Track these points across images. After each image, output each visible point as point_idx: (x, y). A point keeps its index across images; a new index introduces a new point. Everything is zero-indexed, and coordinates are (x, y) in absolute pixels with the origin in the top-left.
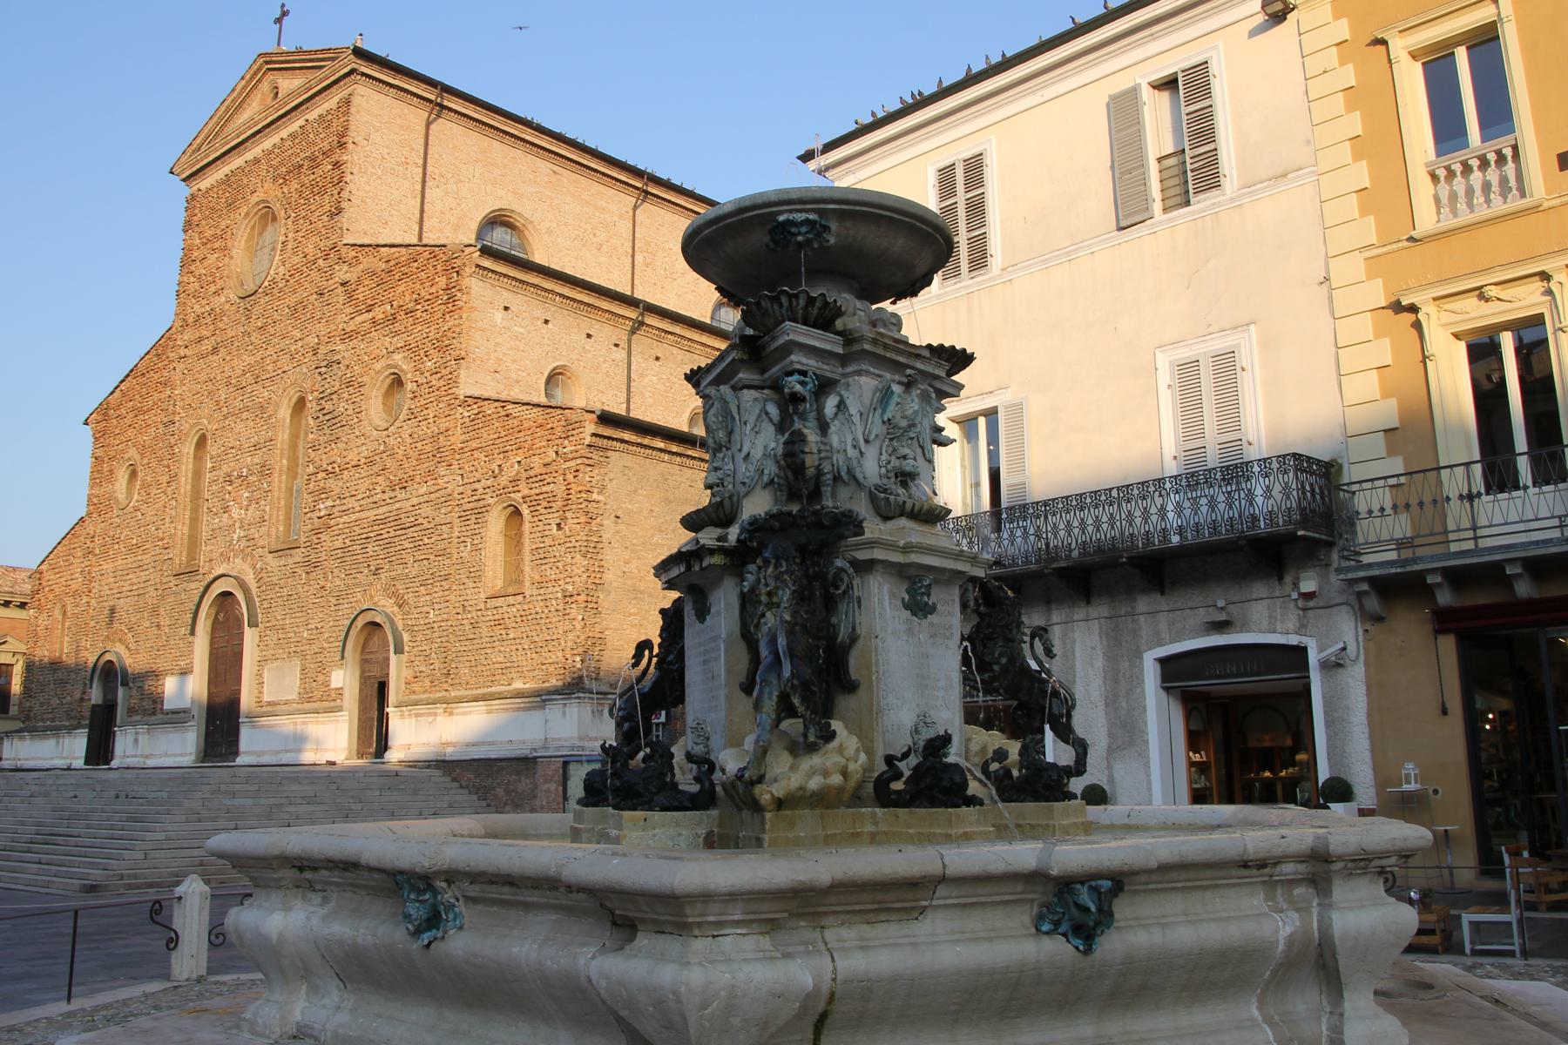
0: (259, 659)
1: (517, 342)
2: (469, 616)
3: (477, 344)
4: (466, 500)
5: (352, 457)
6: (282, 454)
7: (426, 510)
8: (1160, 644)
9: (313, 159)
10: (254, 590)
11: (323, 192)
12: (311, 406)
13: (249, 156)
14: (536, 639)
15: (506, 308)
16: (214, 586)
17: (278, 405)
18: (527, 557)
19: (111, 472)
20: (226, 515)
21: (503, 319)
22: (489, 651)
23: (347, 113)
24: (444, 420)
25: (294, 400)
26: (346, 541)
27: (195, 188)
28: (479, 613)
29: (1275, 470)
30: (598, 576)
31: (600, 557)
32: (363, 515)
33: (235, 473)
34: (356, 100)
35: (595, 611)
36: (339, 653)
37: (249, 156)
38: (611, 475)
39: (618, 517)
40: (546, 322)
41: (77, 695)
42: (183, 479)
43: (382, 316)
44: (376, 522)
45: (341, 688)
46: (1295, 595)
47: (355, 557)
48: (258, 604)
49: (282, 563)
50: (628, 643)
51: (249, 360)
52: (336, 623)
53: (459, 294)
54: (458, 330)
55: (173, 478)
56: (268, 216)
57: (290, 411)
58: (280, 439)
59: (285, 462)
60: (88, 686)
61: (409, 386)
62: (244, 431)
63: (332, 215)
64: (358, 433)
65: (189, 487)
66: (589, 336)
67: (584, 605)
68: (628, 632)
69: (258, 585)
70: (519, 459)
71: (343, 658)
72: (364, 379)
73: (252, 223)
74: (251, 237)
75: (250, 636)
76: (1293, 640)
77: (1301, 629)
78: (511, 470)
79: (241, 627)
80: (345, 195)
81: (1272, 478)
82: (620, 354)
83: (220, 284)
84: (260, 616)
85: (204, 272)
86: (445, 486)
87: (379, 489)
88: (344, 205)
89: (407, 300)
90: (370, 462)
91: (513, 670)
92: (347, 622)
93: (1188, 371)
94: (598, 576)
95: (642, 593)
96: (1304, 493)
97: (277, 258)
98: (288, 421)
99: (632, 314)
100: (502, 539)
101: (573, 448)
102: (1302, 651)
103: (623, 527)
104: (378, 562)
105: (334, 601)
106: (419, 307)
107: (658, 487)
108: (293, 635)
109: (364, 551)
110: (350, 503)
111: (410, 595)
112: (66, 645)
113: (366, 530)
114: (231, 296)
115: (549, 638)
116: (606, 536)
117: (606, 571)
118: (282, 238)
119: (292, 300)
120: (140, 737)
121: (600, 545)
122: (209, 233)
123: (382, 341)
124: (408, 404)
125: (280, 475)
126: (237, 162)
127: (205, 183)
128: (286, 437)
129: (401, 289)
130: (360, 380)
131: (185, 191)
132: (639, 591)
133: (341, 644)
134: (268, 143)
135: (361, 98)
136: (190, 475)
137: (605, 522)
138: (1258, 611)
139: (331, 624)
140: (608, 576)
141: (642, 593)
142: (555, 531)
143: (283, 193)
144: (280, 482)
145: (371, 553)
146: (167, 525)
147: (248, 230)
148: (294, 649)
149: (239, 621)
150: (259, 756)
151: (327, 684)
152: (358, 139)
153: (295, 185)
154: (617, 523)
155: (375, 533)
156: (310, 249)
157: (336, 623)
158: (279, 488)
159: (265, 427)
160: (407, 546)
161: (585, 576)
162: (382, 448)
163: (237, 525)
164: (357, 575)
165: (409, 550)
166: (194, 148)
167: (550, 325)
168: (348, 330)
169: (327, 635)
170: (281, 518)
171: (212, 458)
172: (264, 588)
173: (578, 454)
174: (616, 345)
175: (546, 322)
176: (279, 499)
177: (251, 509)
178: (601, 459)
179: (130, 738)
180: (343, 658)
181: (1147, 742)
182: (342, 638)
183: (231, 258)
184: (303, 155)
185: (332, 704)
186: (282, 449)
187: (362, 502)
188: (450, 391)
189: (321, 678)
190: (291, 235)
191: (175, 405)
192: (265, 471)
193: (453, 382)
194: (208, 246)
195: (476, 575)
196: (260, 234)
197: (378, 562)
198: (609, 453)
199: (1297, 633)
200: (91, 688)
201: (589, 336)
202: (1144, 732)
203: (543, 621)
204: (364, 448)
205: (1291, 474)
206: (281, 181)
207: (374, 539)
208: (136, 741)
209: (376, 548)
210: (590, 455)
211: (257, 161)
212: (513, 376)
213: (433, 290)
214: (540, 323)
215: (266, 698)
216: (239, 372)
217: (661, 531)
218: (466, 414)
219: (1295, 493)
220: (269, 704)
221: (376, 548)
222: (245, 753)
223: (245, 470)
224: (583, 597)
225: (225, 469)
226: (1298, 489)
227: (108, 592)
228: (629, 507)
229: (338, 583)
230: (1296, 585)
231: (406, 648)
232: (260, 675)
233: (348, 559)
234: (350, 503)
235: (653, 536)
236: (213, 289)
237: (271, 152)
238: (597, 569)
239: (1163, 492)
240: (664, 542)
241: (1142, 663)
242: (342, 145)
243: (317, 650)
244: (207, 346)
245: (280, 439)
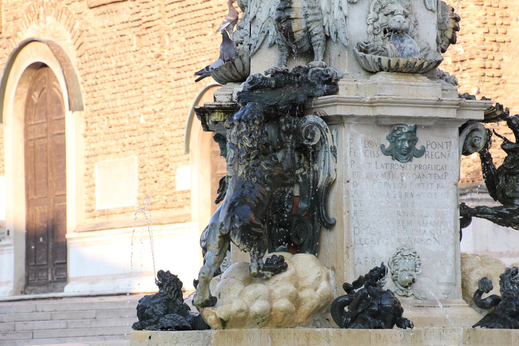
0: (87, 153)
10: (74, 60)
45: (189, 191)
47: (196, 14)
48: (80, 80)
49: (107, 22)
52: (179, 104)
69: (80, 52)
71: (188, 150)
79: (61, 111)
84: (84, 95)
105: (173, 74)
108: (126, 121)
133: (184, 132)
139: (173, 104)
148: (129, 140)
149: (58, 101)
150: (93, 283)
151: (170, 185)
157: (179, 104)
164: (201, 39)
169: (167, 120)
172: (86, 57)
180: (188, 150)
185: (179, 212)
189: (163, 177)
215: (99, 206)
220: (103, 213)
222: (77, 279)
229: (177, 49)
232: (89, 175)
233: (187, 16)
243: (156, 141)
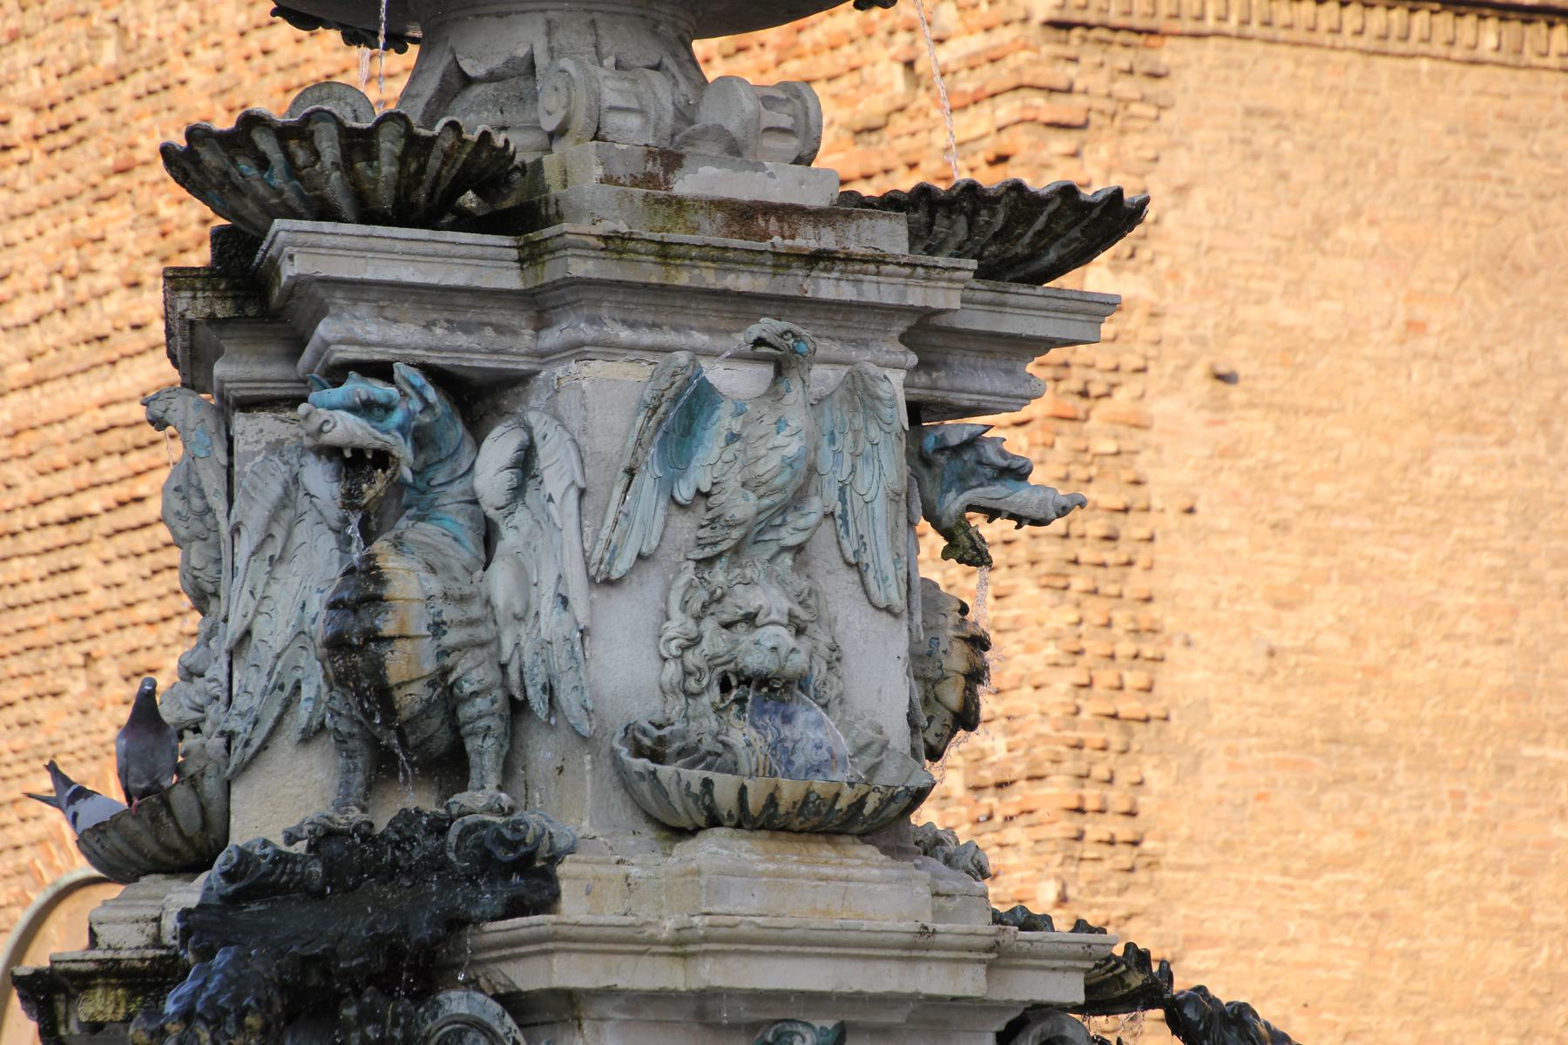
30: (1134, 679)
31: (1137, 582)
32: (44, 402)
35: (1125, 856)
39: (1226, 378)
44: (112, 440)
67: (1069, 825)
68: (1308, 952)
87: (109, 269)
94: (1134, 679)
101: (978, 42)
103: (1257, 425)
104: (131, 638)
107: (1447, 200)
109: (63, 584)
113: (65, 481)
117: (1175, 652)
121: (1133, 528)
132: (1362, 740)
137: (1161, 408)
141: (1381, 749)
145: (97, 597)
154: (1220, 406)
155: (110, 495)
161: (1062, 683)
173: (1001, 76)
178: (1125, 87)
187: (35, 338)
197: (131, 638)
198: (1167, 54)
207: (107, 523)
209: (119, 571)
210: (1062, 74)
217: (1468, 426)
221: (119, 571)
224: (1057, 790)
228: (1288, 317)
235: (1426, 455)
238: (1125, 648)
240: (1488, 486)
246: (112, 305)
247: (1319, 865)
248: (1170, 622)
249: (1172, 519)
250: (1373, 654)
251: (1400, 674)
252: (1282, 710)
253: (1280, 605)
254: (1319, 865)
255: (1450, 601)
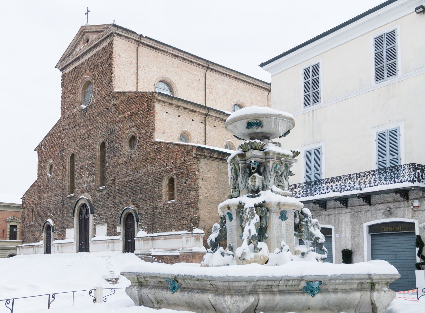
1: (171, 123)
2: (158, 210)
3: (158, 125)
4: (157, 174)
5: (120, 160)
6: (98, 160)
7: (144, 177)
8: (369, 221)
9: (102, 63)
11: (106, 74)
12: (107, 145)
13: (81, 61)
14: (179, 217)
15: (167, 113)
16: (80, 201)
17: (96, 144)
18: (176, 192)
19: (44, 166)
20: (82, 179)
21: (166, 116)
22: (165, 221)
23: (112, 47)
24: (149, 149)
25: (101, 143)
26: (120, 187)
27: (64, 73)
28: (161, 209)
29: (406, 168)
32: (125, 179)
33: (84, 166)
34: (115, 43)
36: (119, 222)
37: (81, 61)
38: (201, 166)
40: (179, 116)
41: (39, 235)
42: (67, 168)
43: (127, 116)
46: (412, 207)
50: (207, 218)
51: (86, 130)
53: (152, 109)
54: (152, 120)
55: (64, 168)
56: (89, 83)
57: (99, 147)
58: (97, 155)
59: (99, 162)
60: (42, 232)
61: (137, 138)
62: (86, 153)
63: (110, 82)
64: (122, 153)
65: (69, 171)
66: (193, 120)
70: (172, 161)
72: (123, 136)
73: (83, 85)
74: (83, 90)
75: (91, 216)
76: (411, 221)
77: (413, 217)
78: (170, 166)
80: (113, 75)
81: (405, 171)
82: (202, 126)
83: (75, 105)
85: (69, 101)
86: (150, 170)
88: (113, 78)
89: (135, 110)
90: (126, 162)
91: (172, 226)
92: (121, 212)
93: (381, 136)
95: (211, 203)
96: (415, 176)
97: (92, 96)
98: (99, 149)
99: (204, 112)
100: (168, 186)
102: (414, 224)
106: (139, 113)
110: (120, 175)
111: (141, 204)
112: (34, 219)
114: (79, 109)
115: (183, 217)
116: (200, 185)
117: (200, 196)
118: (94, 90)
119: (98, 110)
120: (59, 247)
122: (70, 88)
123: (128, 124)
124: (137, 144)
125: (98, 167)
126: (77, 64)
127: (67, 71)
128: (99, 155)
129: (133, 107)
130: (121, 136)
131: (61, 74)
132: (210, 202)
134: (87, 57)
135: (116, 41)
136: (69, 167)
138: (399, 211)
140: (201, 198)
142: (184, 184)
143: (93, 74)
144: (98, 169)
146: (63, 182)
147: (82, 87)
152: (116, 56)
153: (96, 72)
156: (103, 93)
158: (98, 170)
159: (92, 152)
160: (139, 188)
162: (129, 158)
163: (85, 183)
165: (139, 190)
166: (63, 60)
167: (180, 117)
168: (117, 120)
170: (99, 180)
171: (76, 161)
174: (201, 123)
175: (179, 116)
176: (98, 174)
177: (90, 177)
179: (56, 248)
180: (120, 223)
181: (364, 250)
182: (120, 217)
183: (78, 96)
184: (99, 62)
186: (98, 158)
188: (150, 140)
190: (97, 89)
191: (63, 145)
192: (93, 164)
193: (151, 137)
194: (70, 92)
195: (160, 197)
196: (86, 88)
199: (412, 218)
200: (43, 233)
201: (193, 120)
202: (363, 247)
203: (181, 212)
204: (124, 158)
205: (411, 170)
206: (92, 70)
207: (128, 187)
208: (58, 249)
211: (83, 63)
212: (170, 134)
213: (143, 107)
214: (177, 116)
216: (83, 134)
217: (217, 183)
218: (156, 147)
219: (412, 176)
223: (87, 165)
225: (80, 165)
226: (413, 175)
227: (46, 203)
228: (207, 176)
229: (118, 200)
230: (412, 204)
231: (139, 220)
234: (120, 175)
235: (214, 185)
236: (72, 107)
237: (88, 61)
239: (371, 175)
241: (363, 227)
242: (111, 58)
244: (72, 125)
245: (97, 155)
246: (129, 173)
247: (208, 209)
248: (200, 194)
249: (200, 188)
250: (211, 197)
251: (212, 198)
252: (206, 200)
253: (206, 194)
254: (208, 209)
255: (215, 194)
